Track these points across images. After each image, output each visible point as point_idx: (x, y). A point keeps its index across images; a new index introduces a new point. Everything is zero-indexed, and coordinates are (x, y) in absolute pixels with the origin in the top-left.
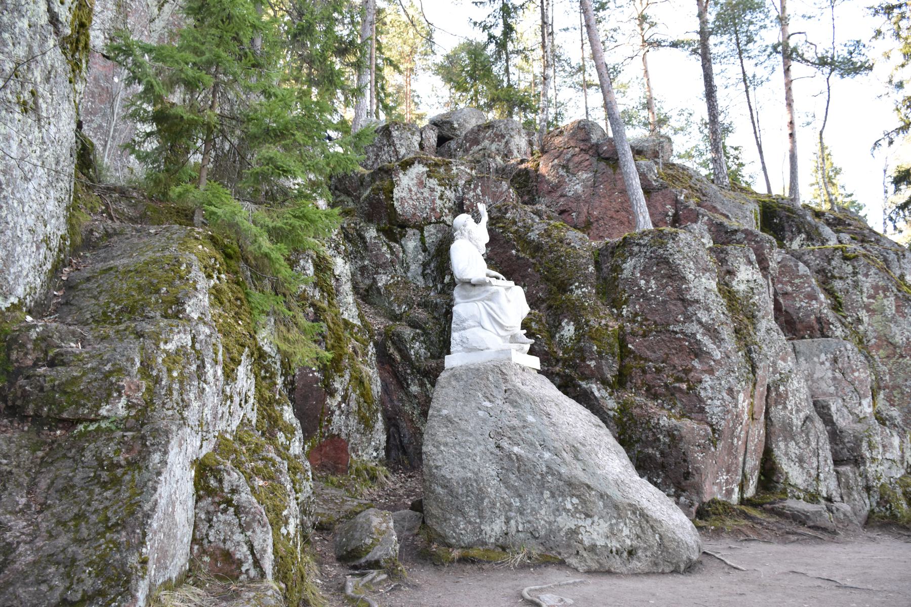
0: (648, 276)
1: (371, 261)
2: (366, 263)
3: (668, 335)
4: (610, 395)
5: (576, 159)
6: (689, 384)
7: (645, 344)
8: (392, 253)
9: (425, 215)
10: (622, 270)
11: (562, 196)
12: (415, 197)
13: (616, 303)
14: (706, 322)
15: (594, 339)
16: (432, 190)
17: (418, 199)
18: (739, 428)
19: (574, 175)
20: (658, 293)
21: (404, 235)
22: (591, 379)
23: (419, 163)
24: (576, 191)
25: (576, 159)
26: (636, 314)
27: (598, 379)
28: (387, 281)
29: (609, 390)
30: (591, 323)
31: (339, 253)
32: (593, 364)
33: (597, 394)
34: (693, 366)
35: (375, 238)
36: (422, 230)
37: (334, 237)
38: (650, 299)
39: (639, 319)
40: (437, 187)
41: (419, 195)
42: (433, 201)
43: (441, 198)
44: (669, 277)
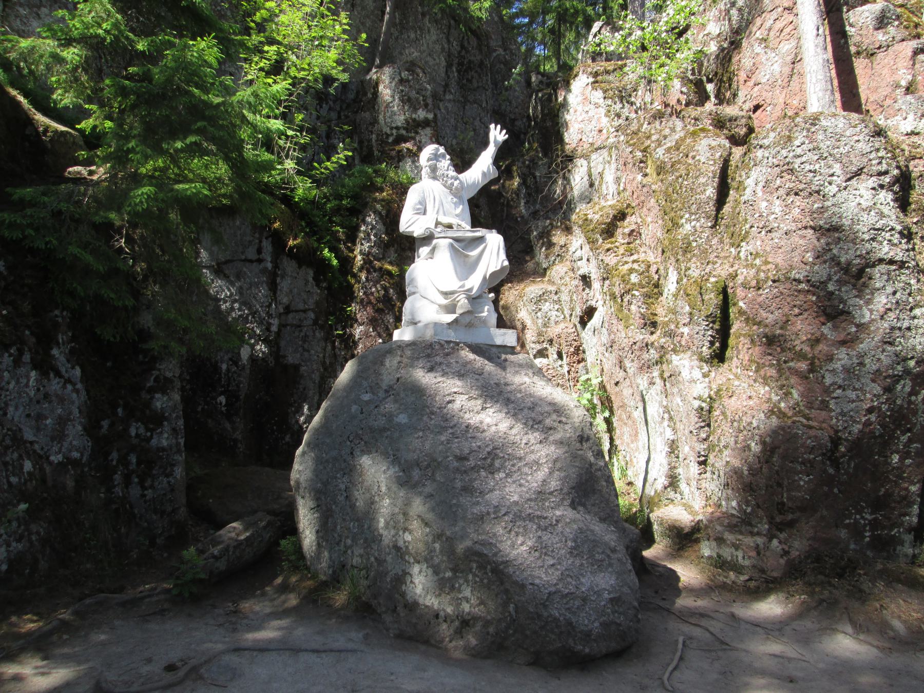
2: (538, 206)
3: (788, 285)
5: (779, 25)
6: (812, 364)
10: (745, 189)
12: (580, 119)
14: (849, 263)
16: (597, 106)
18: (904, 439)
20: (783, 220)
25: (779, 25)
26: (757, 255)
33: (685, 374)
34: (822, 334)
39: (758, 262)
41: (584, 115)
42: (599, 119)
44: (796, 194)
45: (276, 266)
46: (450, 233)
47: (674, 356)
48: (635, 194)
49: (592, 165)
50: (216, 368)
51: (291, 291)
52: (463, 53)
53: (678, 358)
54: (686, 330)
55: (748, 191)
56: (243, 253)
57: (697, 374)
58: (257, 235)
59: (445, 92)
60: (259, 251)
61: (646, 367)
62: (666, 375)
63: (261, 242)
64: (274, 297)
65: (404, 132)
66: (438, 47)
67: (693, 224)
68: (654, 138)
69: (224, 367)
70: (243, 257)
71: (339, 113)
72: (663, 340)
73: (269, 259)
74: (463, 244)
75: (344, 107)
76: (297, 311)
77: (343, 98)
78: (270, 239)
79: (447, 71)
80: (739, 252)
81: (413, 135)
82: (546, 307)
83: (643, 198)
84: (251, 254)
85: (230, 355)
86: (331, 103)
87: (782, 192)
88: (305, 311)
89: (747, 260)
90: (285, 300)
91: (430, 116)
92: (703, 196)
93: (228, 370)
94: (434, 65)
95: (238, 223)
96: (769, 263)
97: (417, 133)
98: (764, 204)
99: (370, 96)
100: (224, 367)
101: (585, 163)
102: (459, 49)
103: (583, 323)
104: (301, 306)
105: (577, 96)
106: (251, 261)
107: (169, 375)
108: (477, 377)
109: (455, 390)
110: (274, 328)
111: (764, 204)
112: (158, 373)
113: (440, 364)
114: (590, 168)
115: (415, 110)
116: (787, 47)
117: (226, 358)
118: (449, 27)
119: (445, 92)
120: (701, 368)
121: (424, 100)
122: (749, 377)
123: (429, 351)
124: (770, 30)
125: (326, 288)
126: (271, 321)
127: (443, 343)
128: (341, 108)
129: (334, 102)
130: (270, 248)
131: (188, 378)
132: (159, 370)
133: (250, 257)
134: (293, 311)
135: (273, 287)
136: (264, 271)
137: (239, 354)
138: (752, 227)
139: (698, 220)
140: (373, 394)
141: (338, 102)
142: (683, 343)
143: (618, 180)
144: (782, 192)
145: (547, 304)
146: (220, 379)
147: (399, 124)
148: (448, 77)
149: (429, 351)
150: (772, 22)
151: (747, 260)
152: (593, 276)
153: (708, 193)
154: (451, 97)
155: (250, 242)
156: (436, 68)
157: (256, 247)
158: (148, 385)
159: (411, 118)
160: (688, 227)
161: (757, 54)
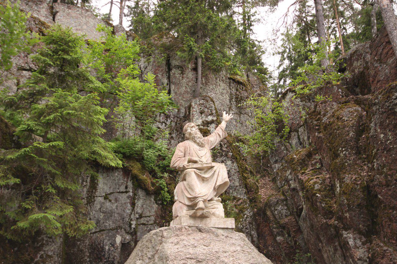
0: (385, 129)
1: (278, 156)
4: (364, 244)
5: (385, 51)
7: (390, 193)
8: (287, 150)
9: (297, 122)
10: (370, 129)
11: (378, 82)
12: (291, 113)
13: (370, 159)
15: (346, 194)
17: (293, 113)
19: (385, 63)
21: (290, 137)
22: (350, 229)
23: (290, 92)
24: (386, 75)
25: (385, 51)
26: (384, 166)
27: (355, 230)
28: (278, 167)
29: (364, 239)
30: (345, 180)
31: (228, 158)
32: (347, 215)
33: (351, 242)
35: (279, 142)
36: (298, 132)
37: (224, 149)
38: (389, 150)
39: (385, 170)
40: (300, 103)
42: (300, 112)
43: (304, 109)
45: (135, 194)
46: (195, 166)
47: (344, 232)
48: (317, 143)
49: (300, 134)
50: (103, 248)
51: (142, 206)
52: (238, 93)
53: (346, 233)
54: (347, 215)
55: (372, 131)
56: (118, 189)
57: (359, 243)
58: (126, 179)
59: (229, 110)
60: (126, 187)
61: (330, 240)
62: (342, 244)
63: (127, 182)
64: (133, 210)
65: (202, 127)
66: (225, 91)
67: (344, 153)
68: (322, 113)
69: (107, 248)
70: (119, 191)
71: (176, 123)
72: (336, 222)
73: (131, 191)
74: (203, 172)
75: (179, 120)
76: (145, 217)
77: (178, 116)
78: (132, 181)
79: (230, 102)
80: (374, 165)
81: (206, 128)
82: (280, 208)
83: (320, 144)
84: (122, 189)
85: (110, 242)
86: (172, 119)
87: (391, 127)
88: (149, 217)
89: (378, 169)
90: (140, 211)
91: (215, 119)
92: (347, 137)
93: (109, 250)
94: (223, 99)
95: (116, 174)
96: (392, 169)
97: (208, 126)
98: (382, 136)
99: (188, 113)
100: (107, 248)
101: (296, 133)
102: (236, 91)
103: (299, 216)
104: (148, 214)
105: (288, 103)
106: (122, 192)
107: (50, 253)
108: (205, 247)
109: (188, 256)
110: (133, 226)
111: (382, 136)
112: (43, 253)
113: (183, 240)
114: (298, 135)
115: (207, 116)
116: (392, 60)
117: (108, 243)
118: (230, 83)
119: (229, 110)
120: (360, 239)
121: (211, 112)
122: (393, 243)
123: (178, 233)
124: (381, 54)
125: (161, 204)
126: (132, 222)
127: (187, 227)
128: (177, 120)
129: (174, 118)
130: (131, 186)
131: (88, 255)
132: (44, 251)
133: (121, 190)
134: (143, 217)
135: (133, 205)
136: (128, 197)
137: (115, 241)
138: (378, 150)
139: (346, 150)
140: (143, 260)
141: (176, 118)
142: (348, 223)
143: (309, 138)
144: (391, 127)
145: (280, 206)
146: (104, 255)
147: (200, 124)
148: (231, 104)
149: (178, 233)
150: (381, 50)
151: (378, 169)
152: (298, 188)
153: (350, 135)
154: (233, 112)
155: (122, 183)
156: (224, 100)
157: (125, 185)
158: (36, 260)
159: (205, 120)
160: (342, 155)
161: (376, 67)
